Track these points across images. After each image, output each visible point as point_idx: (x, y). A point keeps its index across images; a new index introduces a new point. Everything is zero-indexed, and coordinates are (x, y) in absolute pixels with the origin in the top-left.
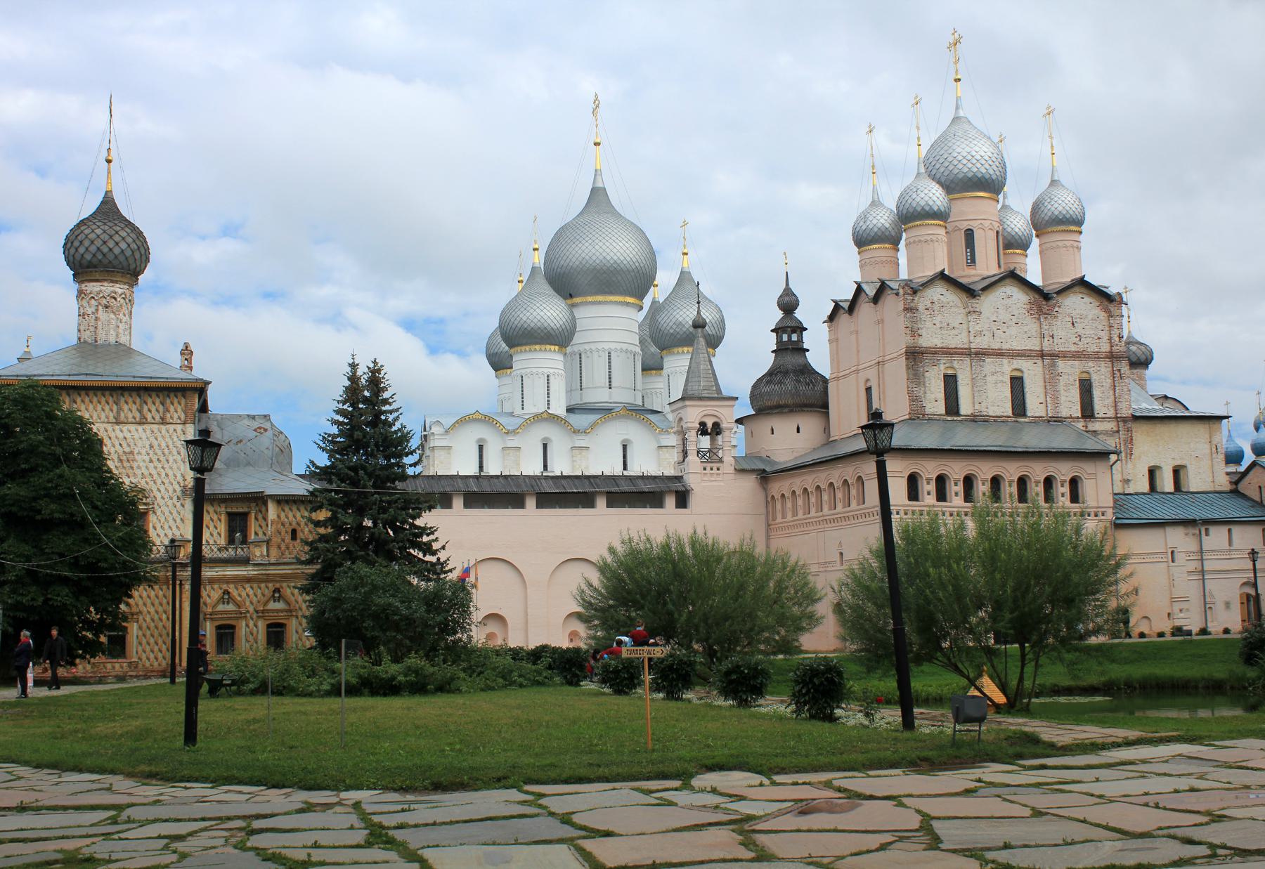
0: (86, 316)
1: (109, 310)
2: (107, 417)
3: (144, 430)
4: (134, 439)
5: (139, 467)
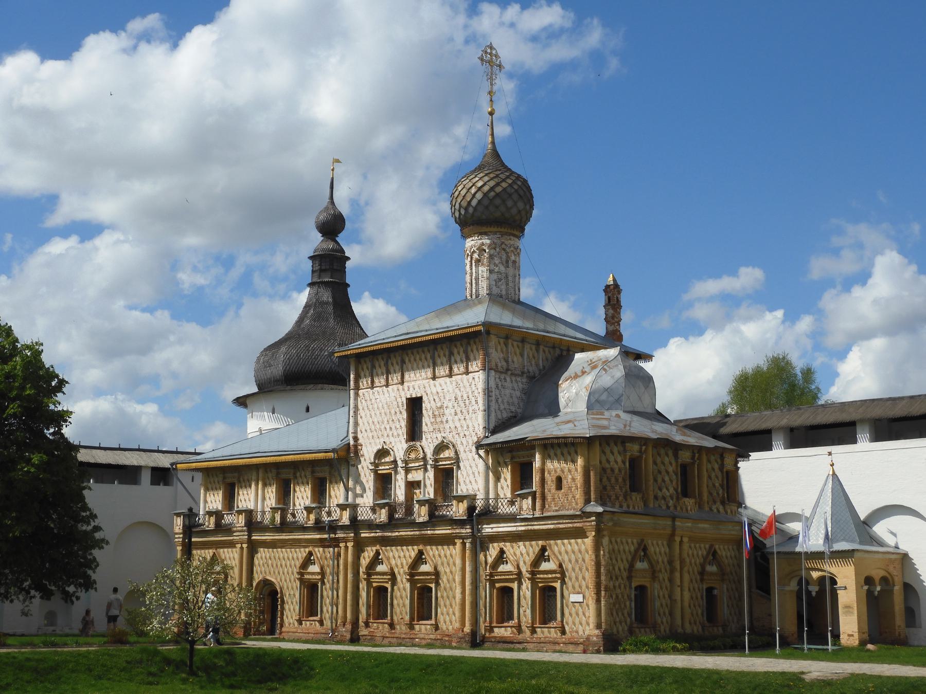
4: (443, 393)
5: (447, 421)
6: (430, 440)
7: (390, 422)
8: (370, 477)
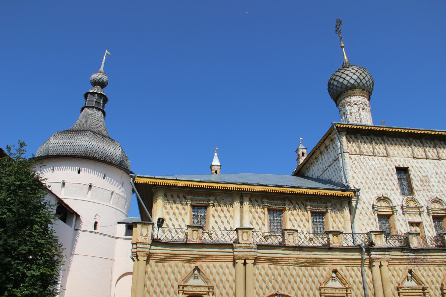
0: (353, 114)
1: (364, 111)
2: (407, 154)
3: (430, 163)
4: (426, 168)
5: (433, 186)
6: (421, 195)
7: (384, 179)
8: (371, 216)
